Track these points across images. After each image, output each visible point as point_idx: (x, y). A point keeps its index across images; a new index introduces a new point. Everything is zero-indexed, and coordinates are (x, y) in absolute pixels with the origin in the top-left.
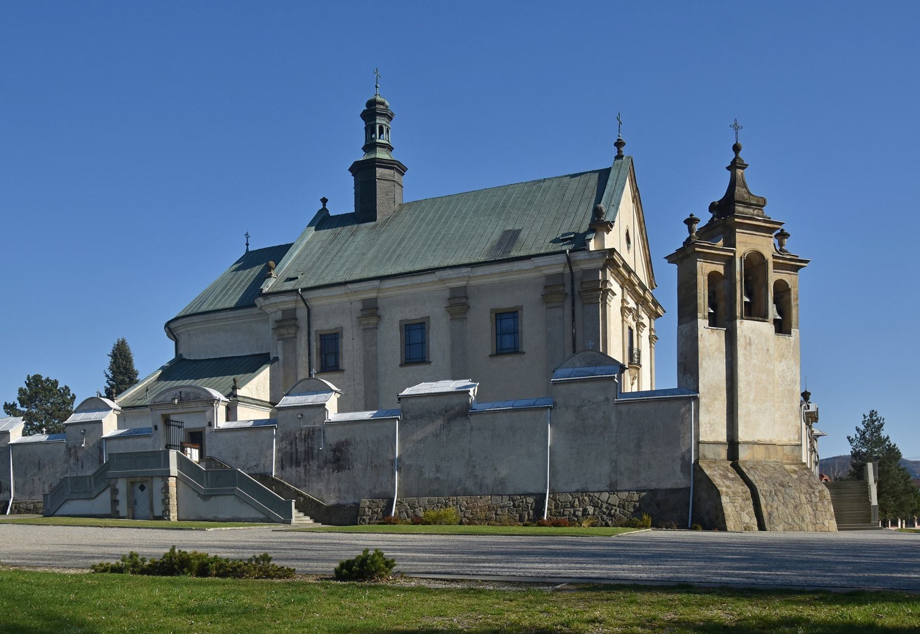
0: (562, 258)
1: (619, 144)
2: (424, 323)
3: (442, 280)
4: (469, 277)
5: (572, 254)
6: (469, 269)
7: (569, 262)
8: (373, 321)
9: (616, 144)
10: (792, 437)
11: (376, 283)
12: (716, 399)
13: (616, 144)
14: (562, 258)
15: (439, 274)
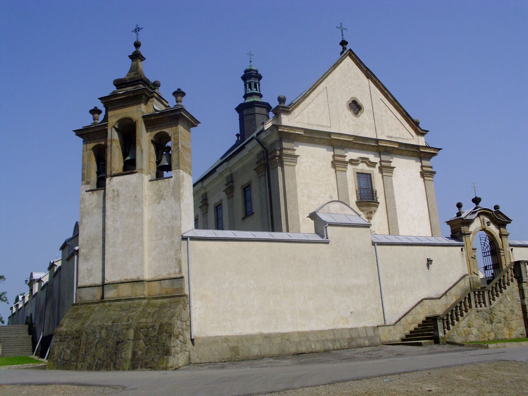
0: (255, 142)
1: (344, 43)
2: (220, 204)
3: (220, 174)
4: (229, 168)
5: (259, 136)
6: (225, 164)
7: (260, 143)
8: (204, 208)
9: (341, 44)
10: (172, 271)
11: (200, 184)
12: (93, 248)
13: (341, 44)
14: (255, 142)
15: (219, 170)
